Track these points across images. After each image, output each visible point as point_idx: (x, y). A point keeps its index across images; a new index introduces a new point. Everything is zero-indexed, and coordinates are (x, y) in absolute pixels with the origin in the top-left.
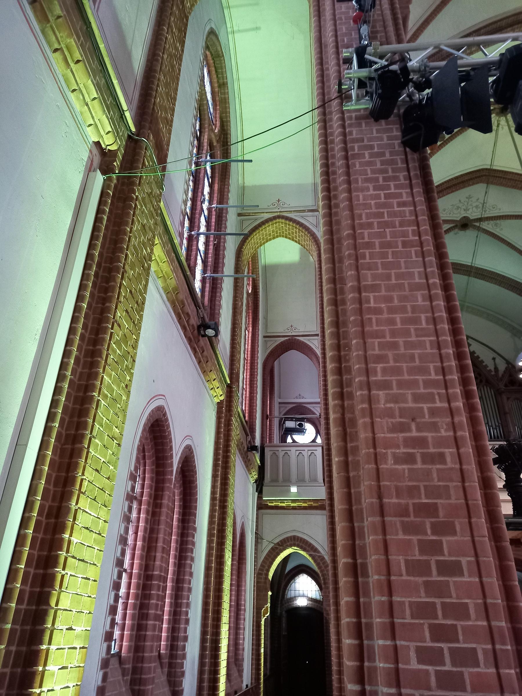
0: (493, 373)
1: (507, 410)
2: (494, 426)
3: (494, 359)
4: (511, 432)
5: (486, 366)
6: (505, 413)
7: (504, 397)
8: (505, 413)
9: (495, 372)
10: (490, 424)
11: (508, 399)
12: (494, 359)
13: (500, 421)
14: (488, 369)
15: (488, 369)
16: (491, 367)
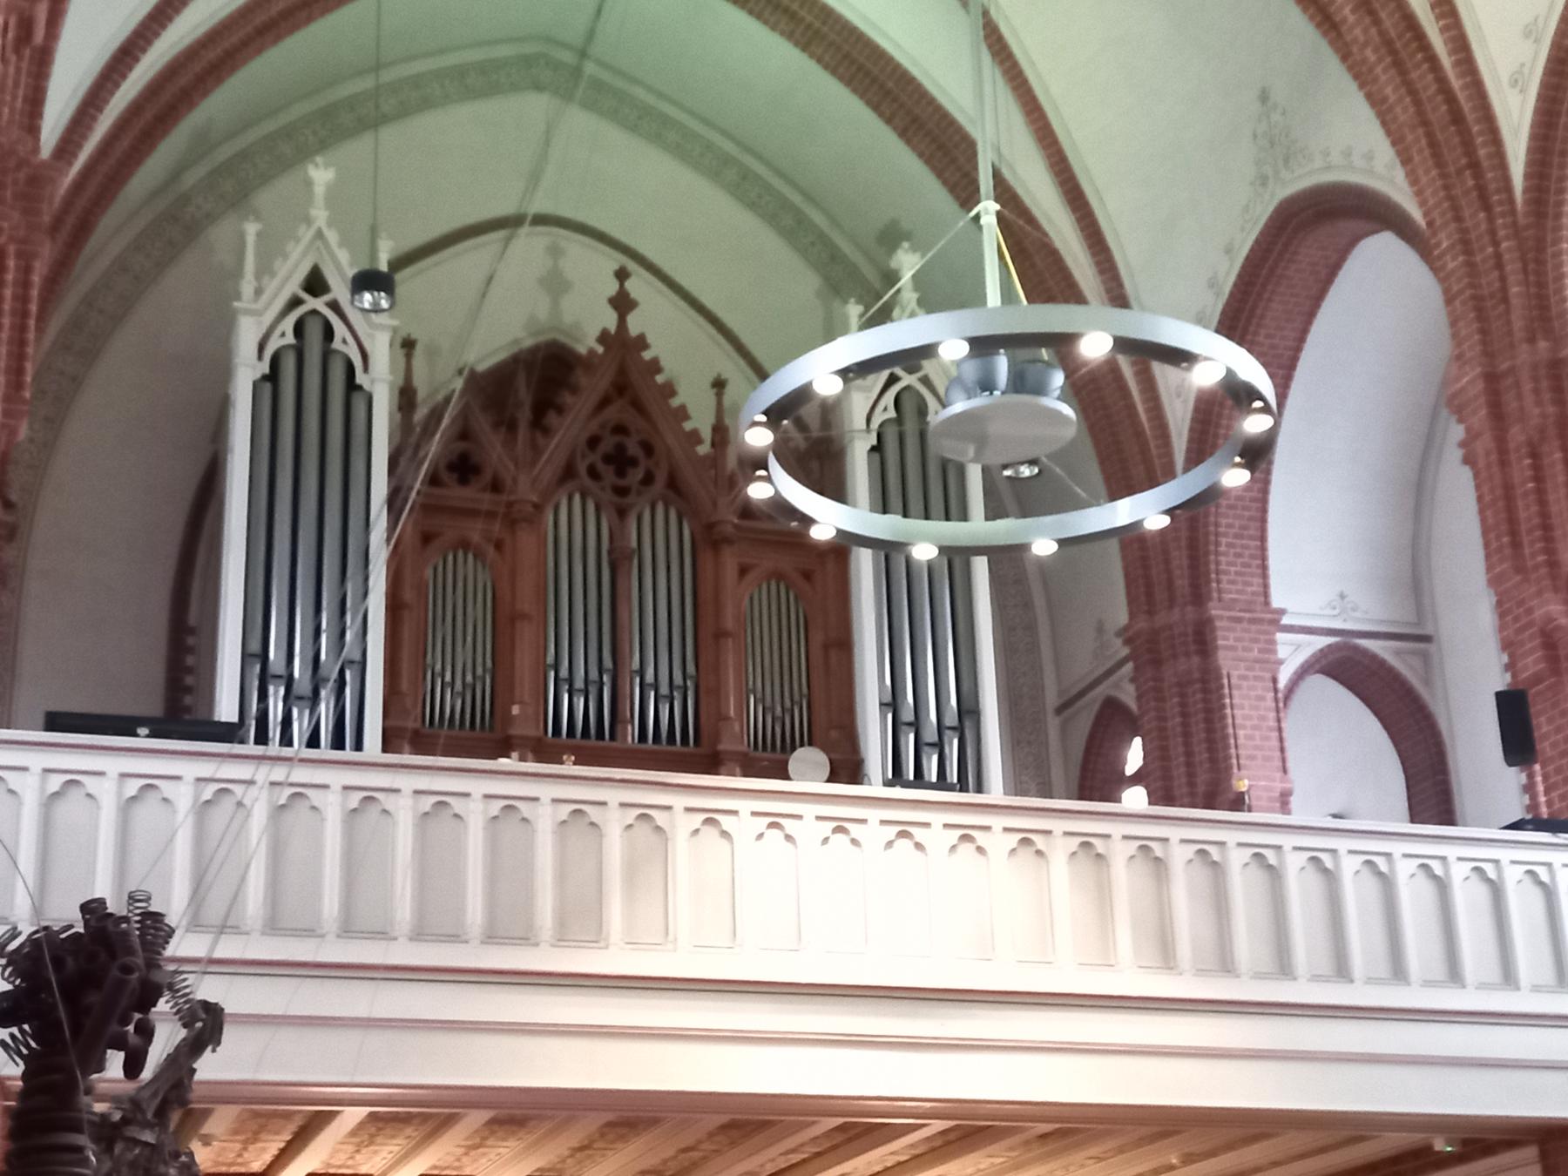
0: (704, 449)
1: (729, 623)
2: (664, 690)
3: (719, 385)
4: (727, 718)
5: (682, 413)
6: (720, 635)
7: (730, 561)
8: (720, 635)
9: (713, 445)
10: (650, 677)
11: (743, 571)
12: (719, 385)
13: (691, 669)
14: (688, 426)
15: (688, 426)
16: (701, 420)
